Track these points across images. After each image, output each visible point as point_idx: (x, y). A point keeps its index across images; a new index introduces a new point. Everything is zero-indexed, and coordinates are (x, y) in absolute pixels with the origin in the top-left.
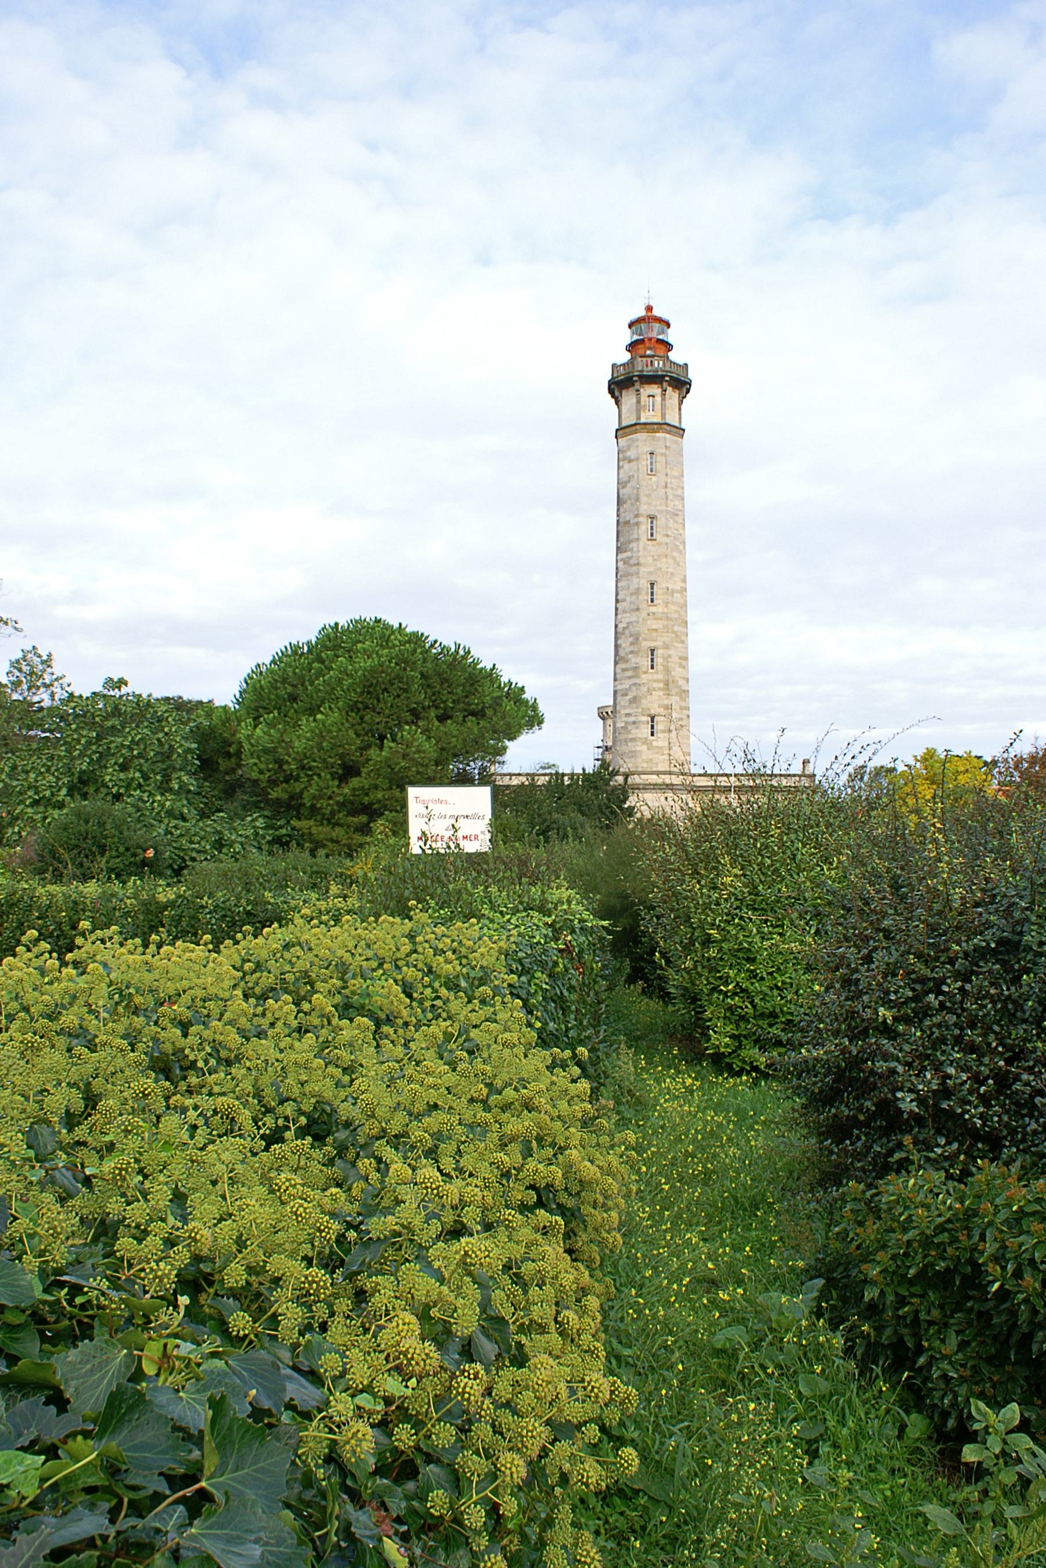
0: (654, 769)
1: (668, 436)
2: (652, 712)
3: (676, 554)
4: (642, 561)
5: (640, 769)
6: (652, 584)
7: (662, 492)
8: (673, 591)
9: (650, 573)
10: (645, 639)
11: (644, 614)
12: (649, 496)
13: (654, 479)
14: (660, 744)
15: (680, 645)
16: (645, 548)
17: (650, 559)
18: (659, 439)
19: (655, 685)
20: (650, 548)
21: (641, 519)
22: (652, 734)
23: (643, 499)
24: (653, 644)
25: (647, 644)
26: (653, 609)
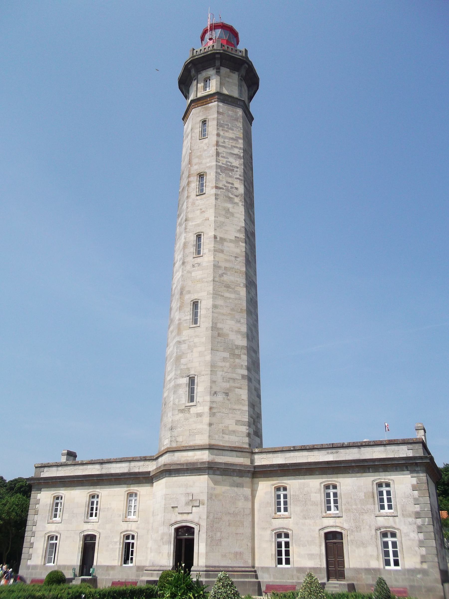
0: (191, 443)
1: (221, 104)
2: (192, 373)
3: (229, 206)
4: (190, 216)
5: (174, 445)
6: (199, 237)
7: (213, 150)
8: (223, 240)
9: (198, 225)
10: (189, 292)
11: (188, 267)
12: (200, 157)
13: (206, 141)
14: (199, 409)
15: (233, 296)
16: (193, 204)
17: (198, 212)
18: (211, 108)
19: (196, 340)
20: (197, 203)
21: (192, 179)
22: (192, 399)
23: (195, 161)
24: (195, 296)
25: (189, 298)
26: (199, 260)
